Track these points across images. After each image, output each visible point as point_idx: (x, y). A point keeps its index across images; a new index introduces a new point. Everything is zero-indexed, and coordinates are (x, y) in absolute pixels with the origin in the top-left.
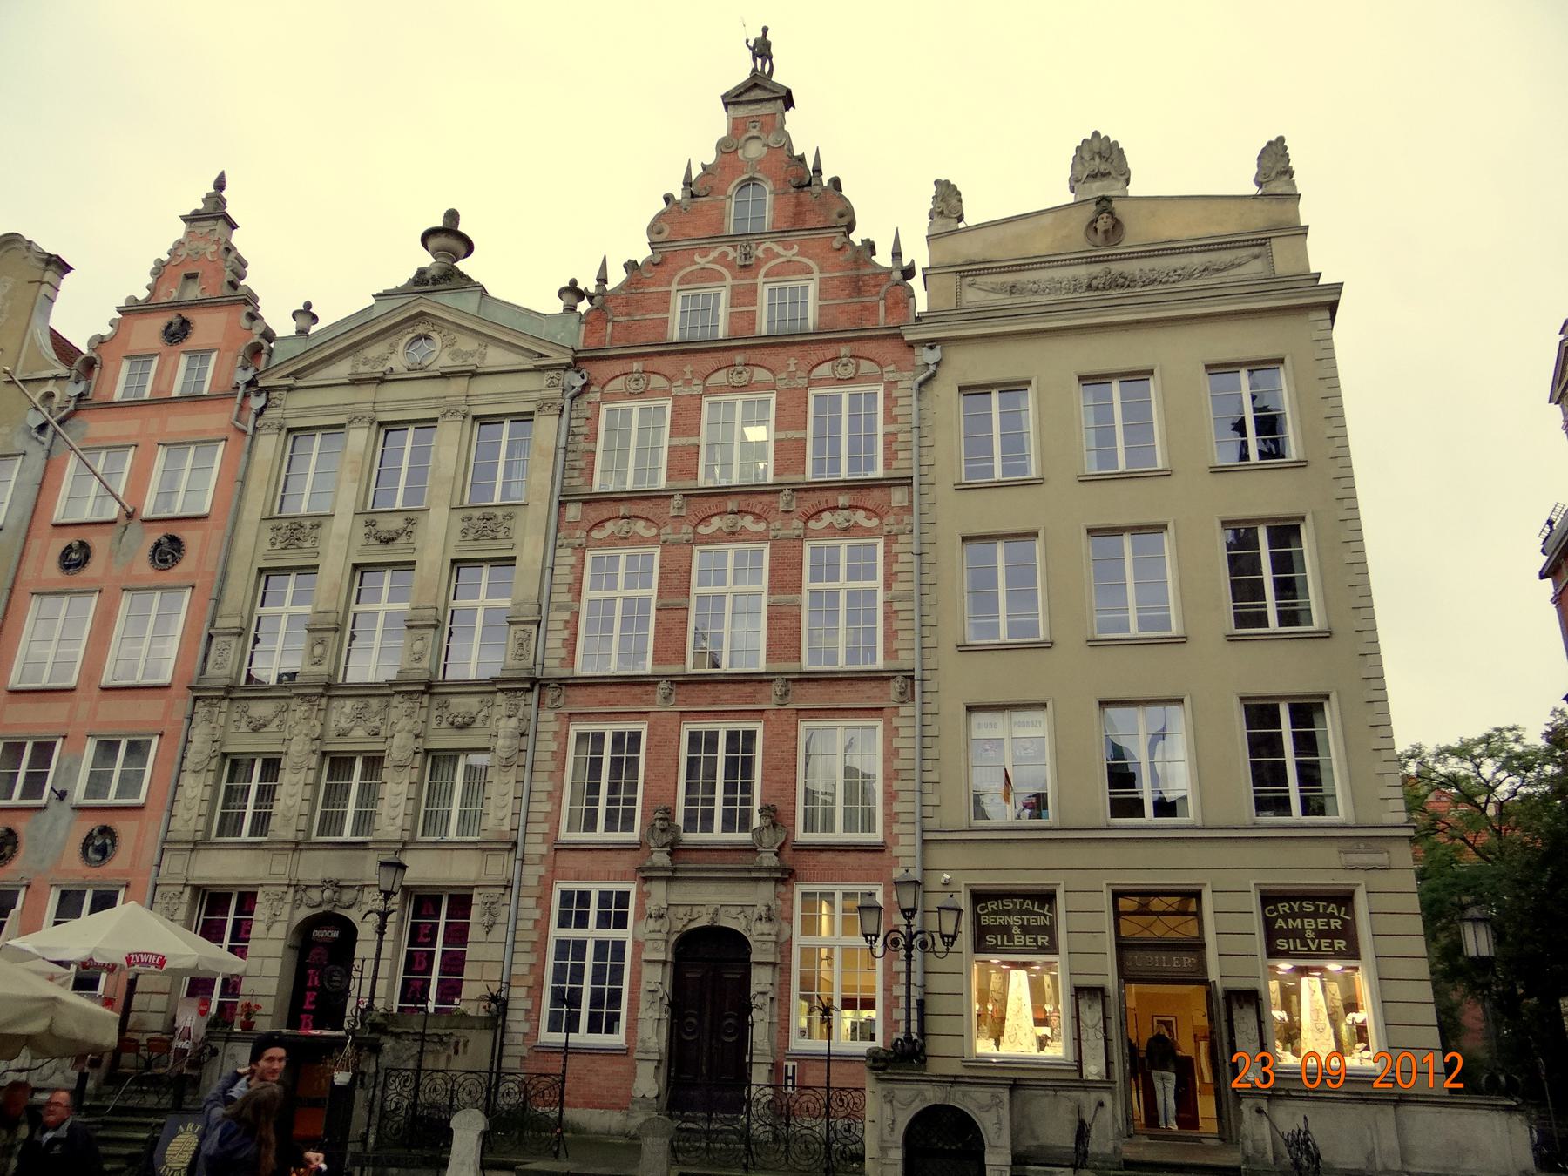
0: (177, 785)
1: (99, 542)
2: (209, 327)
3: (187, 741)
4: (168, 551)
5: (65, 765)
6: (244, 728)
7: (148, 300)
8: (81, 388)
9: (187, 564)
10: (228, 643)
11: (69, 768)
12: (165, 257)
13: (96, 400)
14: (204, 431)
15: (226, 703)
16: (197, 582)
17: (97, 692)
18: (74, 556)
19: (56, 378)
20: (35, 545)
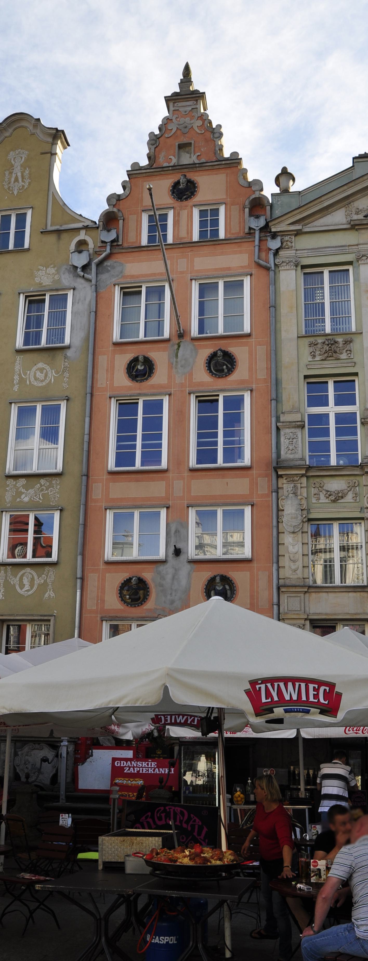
0: (278, 544)
1: (160, 358)
2: (210, 187)
3: (278, 510)
4: (221, 363)
5: (173, 530)
6: (323, 499)
7: (150, 166)
8: (113, 235)
9: (241, 372)
10: (294, 433)
11: (177, 531)
12: (157, 132)
13: (125, 245)
14: (229, 269)
15: (304, 480)
16: (254, 387)
17: (186, 474)
18: (140, 367)
19: (86, 228)
20: (103, 360)
